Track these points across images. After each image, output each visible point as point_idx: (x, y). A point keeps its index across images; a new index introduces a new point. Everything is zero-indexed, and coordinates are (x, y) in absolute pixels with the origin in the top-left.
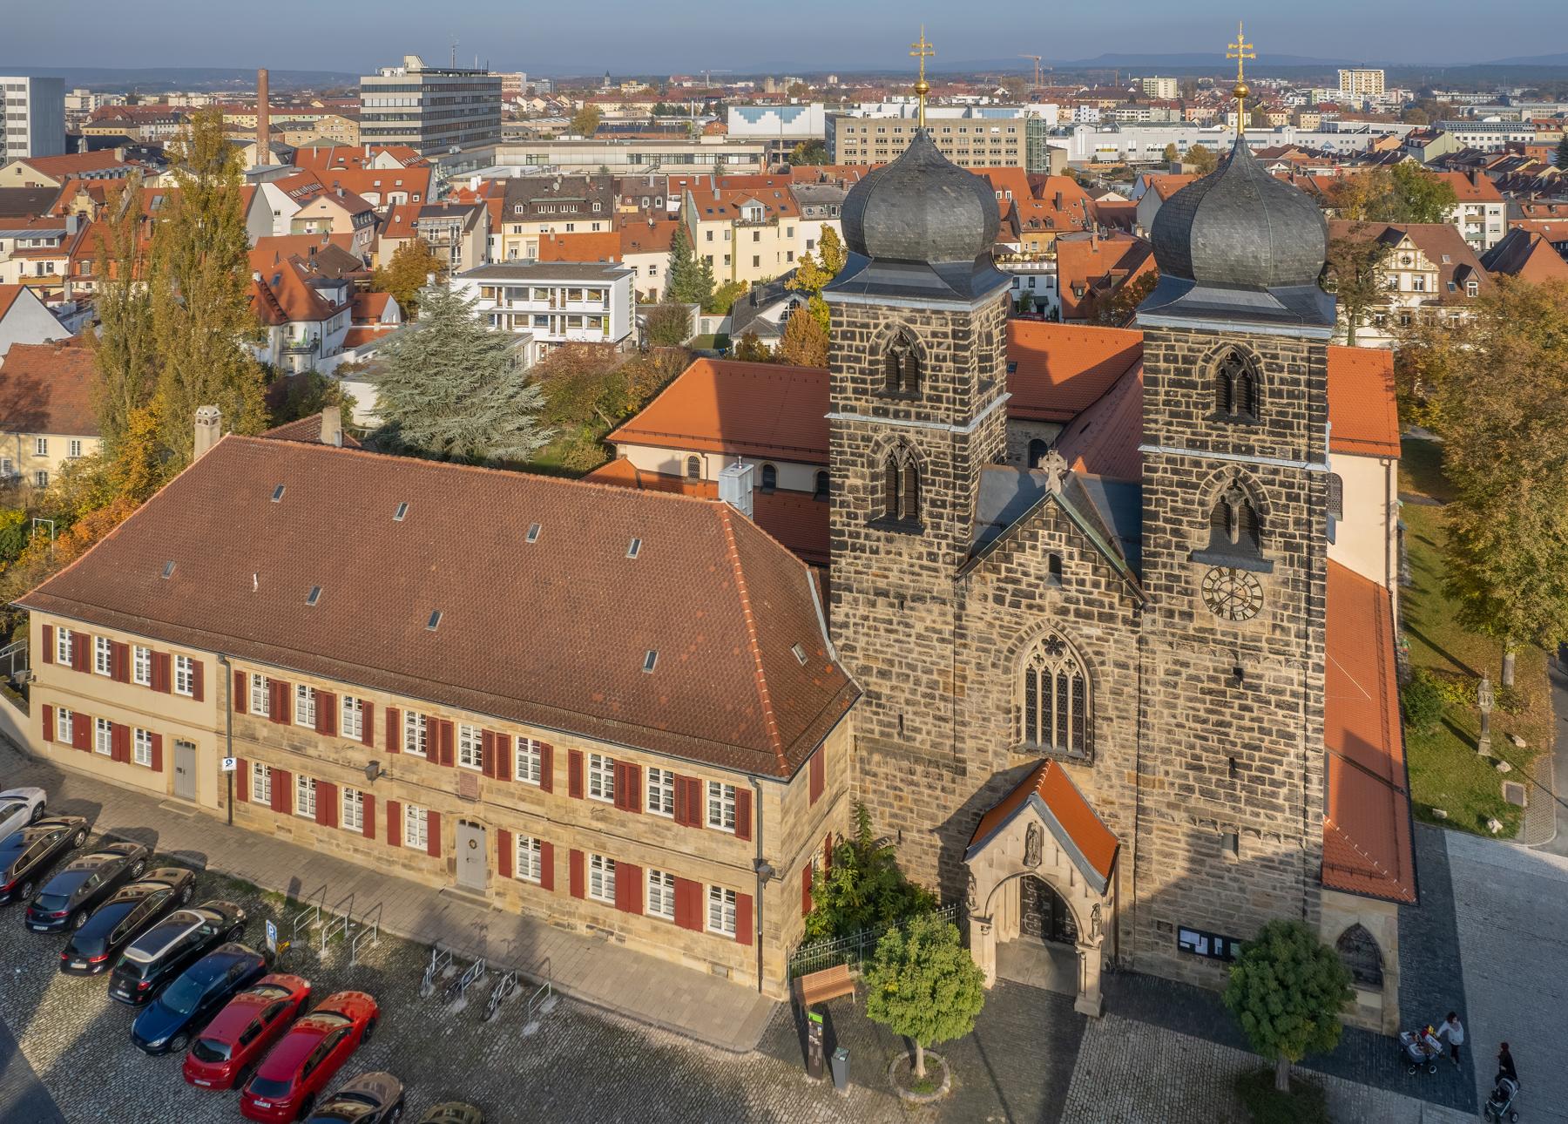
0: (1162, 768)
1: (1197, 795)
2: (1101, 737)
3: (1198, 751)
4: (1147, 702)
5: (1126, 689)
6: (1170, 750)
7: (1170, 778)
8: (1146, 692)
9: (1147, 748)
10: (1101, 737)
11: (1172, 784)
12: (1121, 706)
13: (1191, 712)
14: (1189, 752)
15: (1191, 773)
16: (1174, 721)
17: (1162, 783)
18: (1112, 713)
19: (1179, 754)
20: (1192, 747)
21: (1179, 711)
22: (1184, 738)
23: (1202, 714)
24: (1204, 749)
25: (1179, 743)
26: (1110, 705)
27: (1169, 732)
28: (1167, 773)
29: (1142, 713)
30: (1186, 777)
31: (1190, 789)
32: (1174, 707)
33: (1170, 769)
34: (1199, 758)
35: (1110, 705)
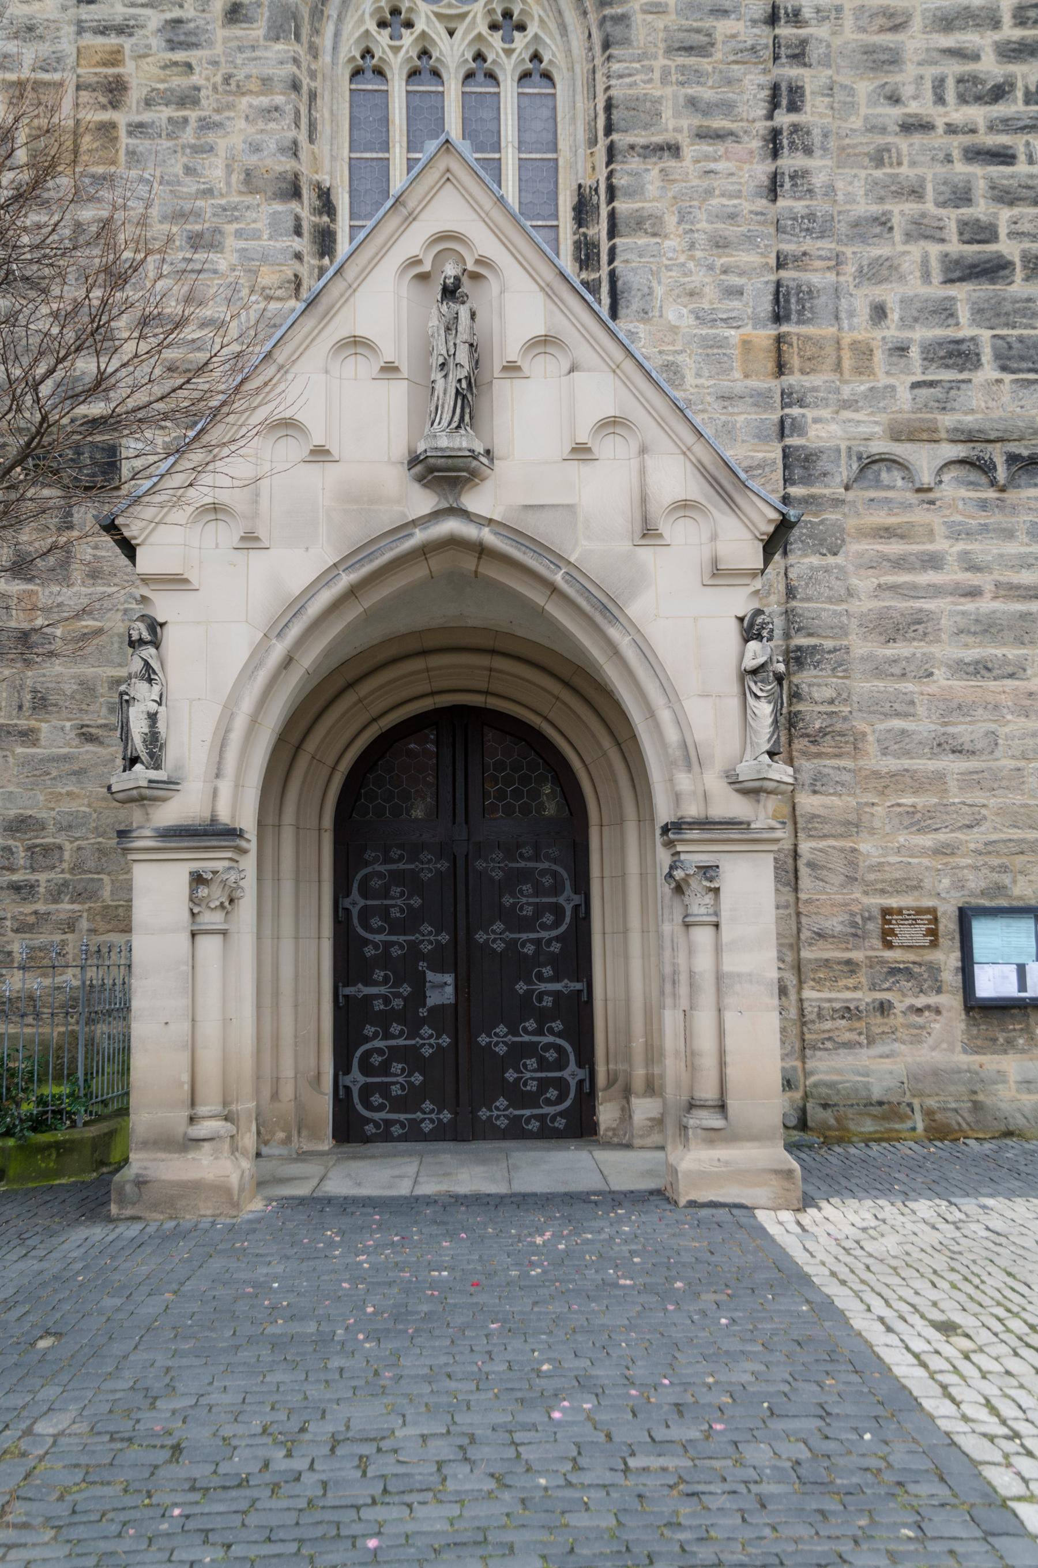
0: (860, 301)
1: (988, 371)
2: (639, 223)
3: (981, 209)
4: (799, 56)
5: (723, 27)
6: (884, 222)
7: (891, 331)
8: (796, 17)
9: (813, 225)
10: (639, 223)
11: (901, 350)
12: (706, 94)
13: (954, 68)
14: (951, 217)
15: (963, 293)
16: (894, 113)
17: (864, 352)
18: (675, 124)
19: (923, 230)
20: (962, 197)
21: (905, 78)
22: (931, 174)
23: (991, 68)
24: (1005, 197)
25: (916, 193)
26: (669, 97)
27: (879, 158)
28: (879, 312)
29: (783, 97)
30: (946, 312)
31: (960, 355)
32: (893, 60)
33: (890, 294)
34: (981, 232)
35: (669, 97)
